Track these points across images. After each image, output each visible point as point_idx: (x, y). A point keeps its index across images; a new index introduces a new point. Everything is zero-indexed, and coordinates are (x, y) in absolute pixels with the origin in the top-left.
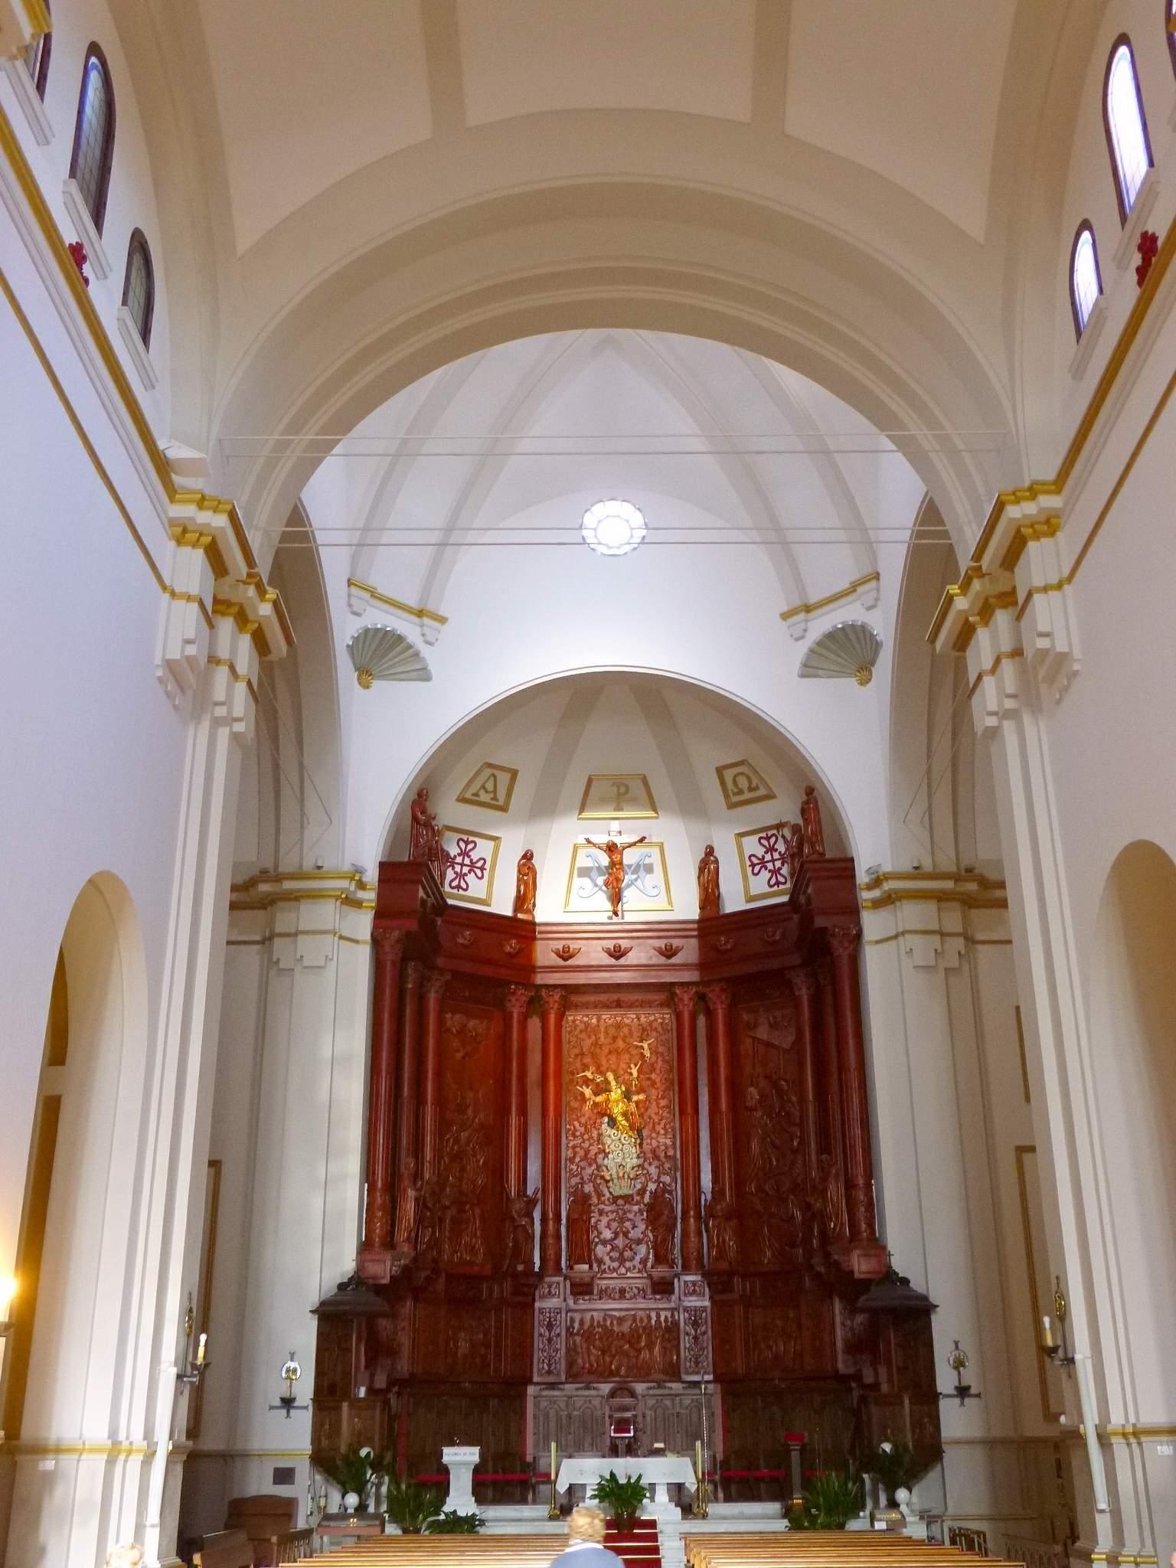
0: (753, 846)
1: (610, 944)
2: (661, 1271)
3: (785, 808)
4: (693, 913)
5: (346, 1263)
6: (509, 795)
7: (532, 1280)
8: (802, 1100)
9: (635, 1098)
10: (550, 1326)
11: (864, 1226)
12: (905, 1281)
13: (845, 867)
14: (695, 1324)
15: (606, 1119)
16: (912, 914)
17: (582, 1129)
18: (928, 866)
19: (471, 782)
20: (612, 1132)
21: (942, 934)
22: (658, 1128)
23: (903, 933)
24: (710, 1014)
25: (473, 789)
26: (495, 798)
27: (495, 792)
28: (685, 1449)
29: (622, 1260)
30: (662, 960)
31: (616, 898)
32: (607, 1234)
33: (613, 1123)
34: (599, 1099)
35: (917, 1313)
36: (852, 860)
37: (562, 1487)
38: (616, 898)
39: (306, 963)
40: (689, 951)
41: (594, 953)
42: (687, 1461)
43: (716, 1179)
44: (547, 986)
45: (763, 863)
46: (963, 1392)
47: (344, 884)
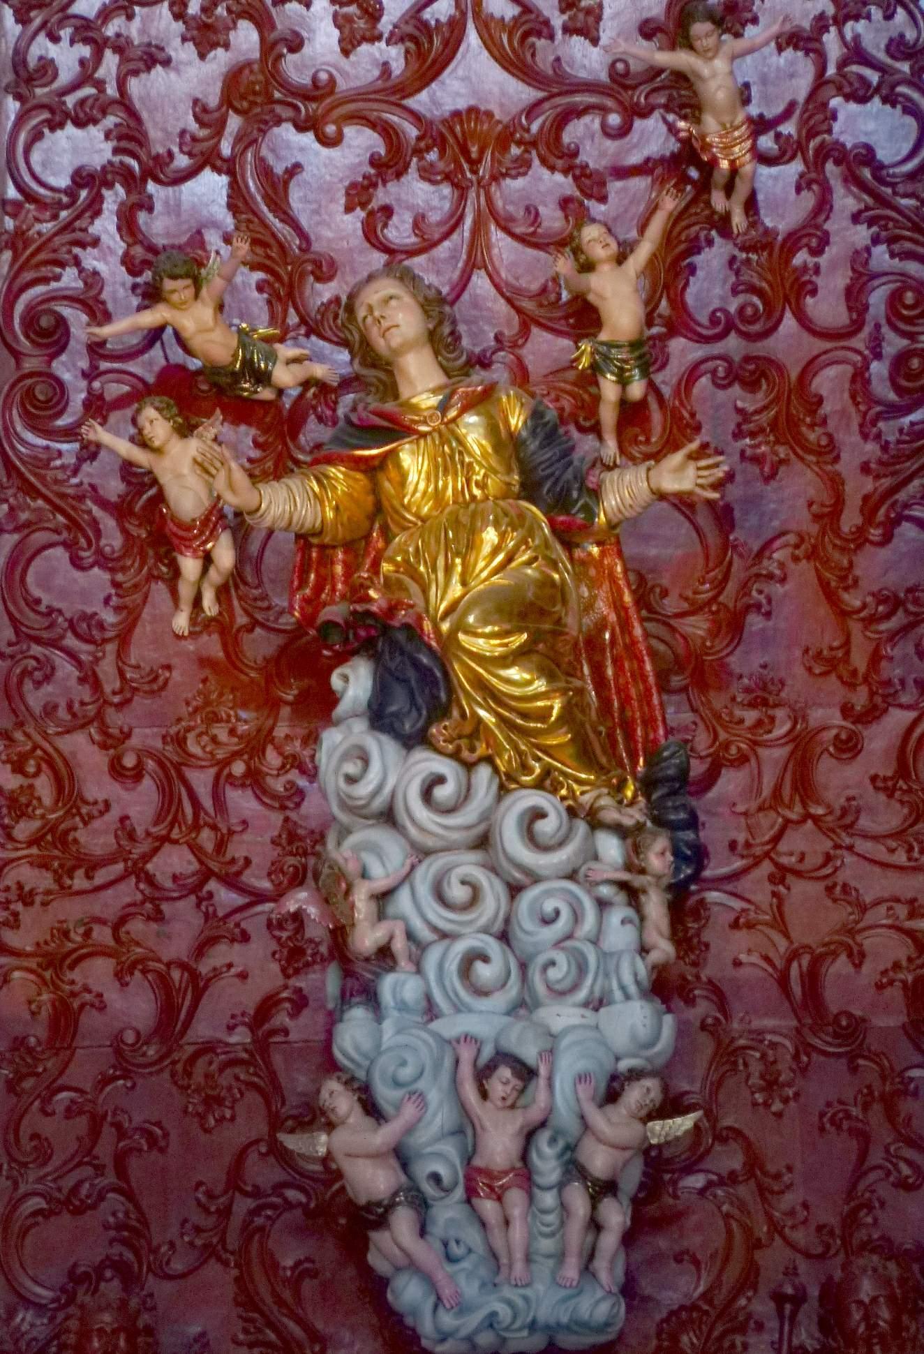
9: (622, 491)
15: (355, 683)
17: (140, 802)
20: (394, 770)
22: (838, 780)
33: (420, 695)
34: (290, 503)
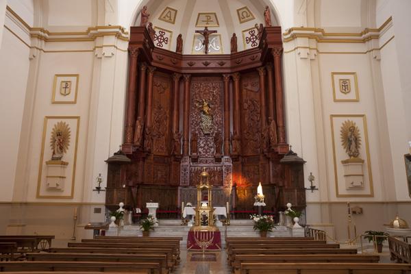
0: (247, 35)
1: (204, 61)
2: (218, 155)
3: (259, 21)
4: (229, 52)
5: (117, 149)
6: (174, 20)
7: (180, 157)
8: (261, 106)
10: (185, 170)
11: (282, 139)
12: (295, 154)
13: (279, 29)
14: (228, 170)
16: (300, 42)
18: (305, 26)
19: (163, 13)
21: (310, 49)
23: (297, 48)
24: (233, 82)
25: (164, 16)
26: (170, 19)
27: (170, 17)
28: (225, 205)
29: (207, 152)
30: (220, 66)
31: (206, 43)
32: (202, 145)
35: (298, 165)
36: (280, 27)
37: (184, 216)
38: (206, 43)
39: (106, 55)
40: (228, 64)
41: (199, 64)
42: (225, 208)
43: (234, 128)
44: (185, 74)
45: (250, 39)
46: (313, 188)
47: (118, 30)
